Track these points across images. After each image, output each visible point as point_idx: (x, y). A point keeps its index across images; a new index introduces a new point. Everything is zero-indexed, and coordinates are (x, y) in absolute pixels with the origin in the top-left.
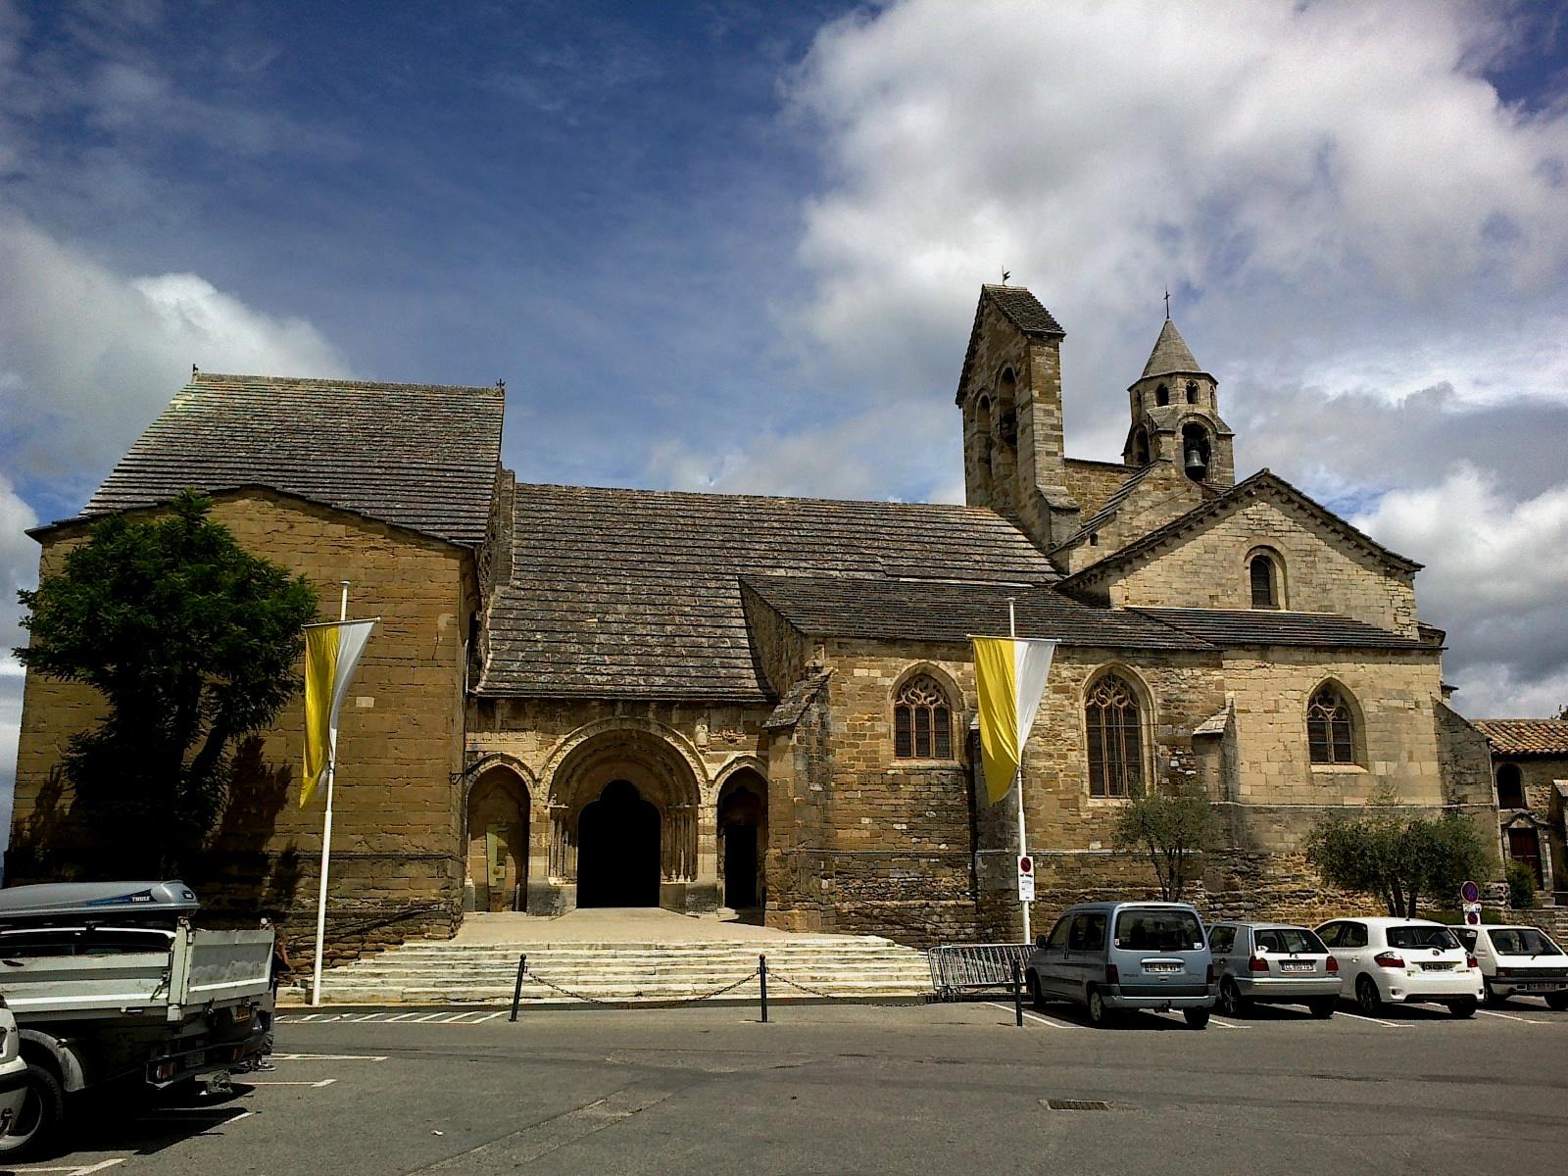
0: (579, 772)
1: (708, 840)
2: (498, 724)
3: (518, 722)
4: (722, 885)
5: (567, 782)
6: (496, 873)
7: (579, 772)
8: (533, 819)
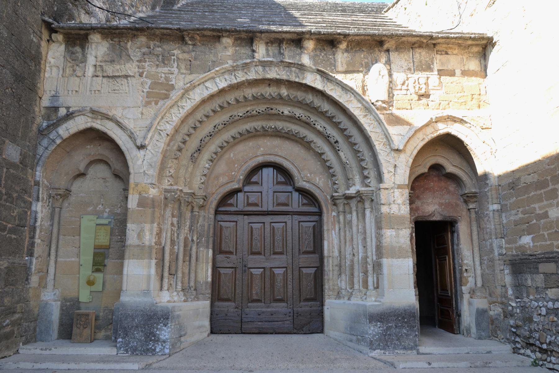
0: (213, 147)
1: (397, 236)
2: (90, 71)
3: (118, 67)
4: (417, 306)
5: (193, 159)
6: (90, 283)
7: (213, 147)
8: (133, 202)
